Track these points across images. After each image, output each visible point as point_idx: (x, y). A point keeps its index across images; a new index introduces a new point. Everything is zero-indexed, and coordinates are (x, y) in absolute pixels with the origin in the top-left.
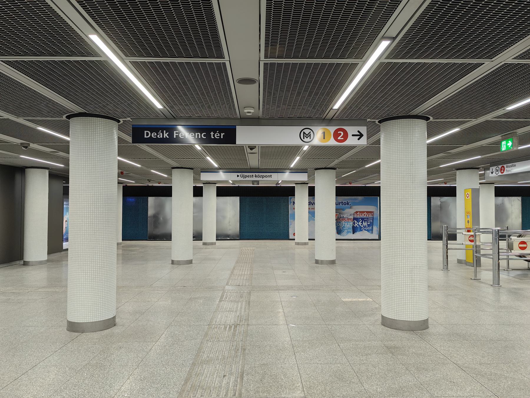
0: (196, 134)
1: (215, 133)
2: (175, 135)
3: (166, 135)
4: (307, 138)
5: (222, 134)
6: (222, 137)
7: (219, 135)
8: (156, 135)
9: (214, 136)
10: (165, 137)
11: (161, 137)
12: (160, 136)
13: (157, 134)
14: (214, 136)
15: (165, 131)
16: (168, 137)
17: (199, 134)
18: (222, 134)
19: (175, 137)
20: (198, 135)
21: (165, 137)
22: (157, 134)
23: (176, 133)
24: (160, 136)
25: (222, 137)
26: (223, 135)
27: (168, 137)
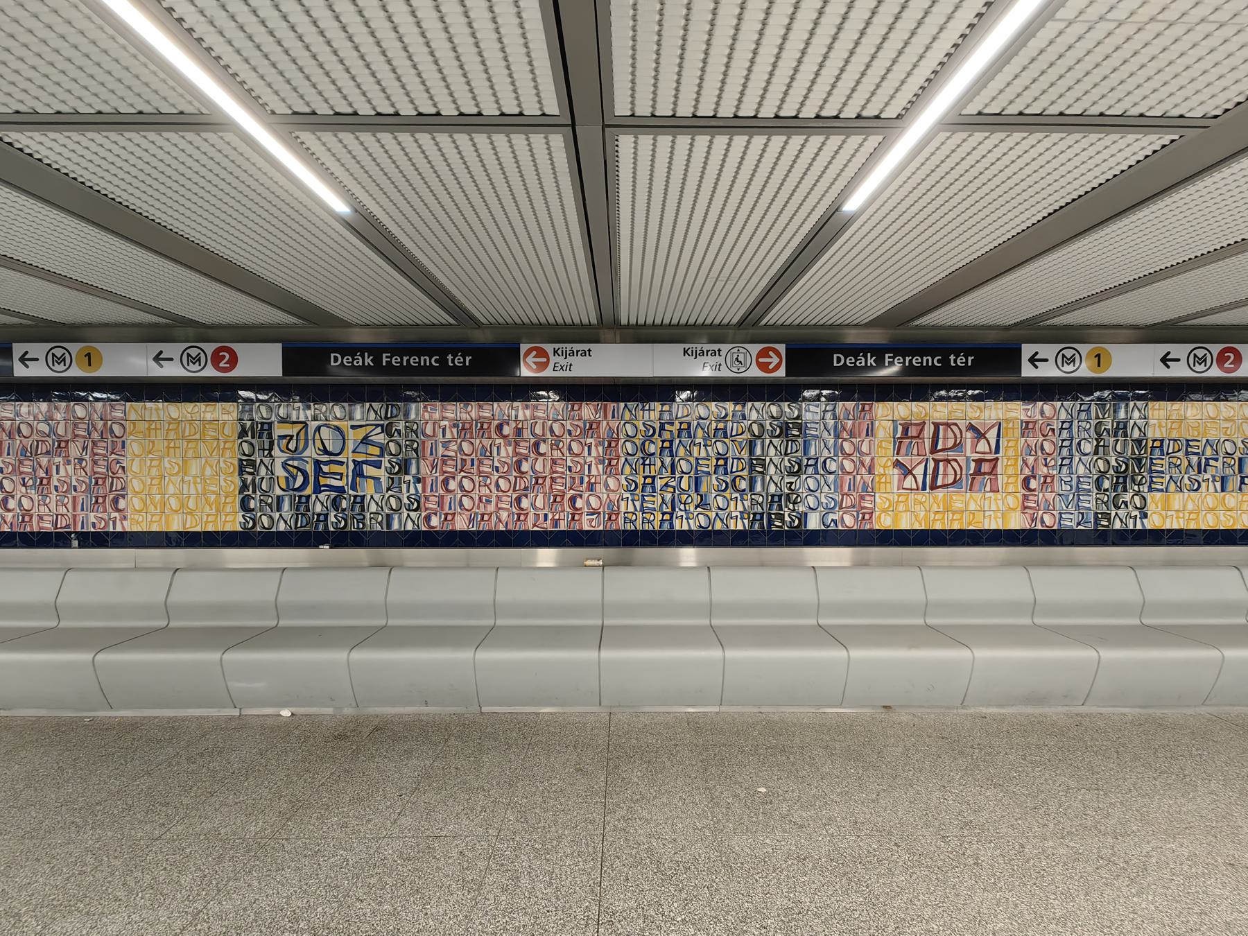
0: (422, 358)
1: (455, 356)
2: (384, 360)
3: (368, 361)
4: (194, 363)
5: (468, 359)
6: (467, 364)
7: (462, 360)
8: (351, 360)
9: (453, 361)
10: (366, 364)
11: (361, 364)
12: (358, 363)
13: (353, 360)
14: (453, 361)
15: (366, 354)
16: (372, 364)
17: (427, 358)
18: (468, 359)
19: (384, 364)
20: (425, 360)
21: (366, 364)
22: (353, 360)
23: (387, 357)
24: (358, 363)
25: (467, 364)
26: (470, 360)
27: (372, 364)
